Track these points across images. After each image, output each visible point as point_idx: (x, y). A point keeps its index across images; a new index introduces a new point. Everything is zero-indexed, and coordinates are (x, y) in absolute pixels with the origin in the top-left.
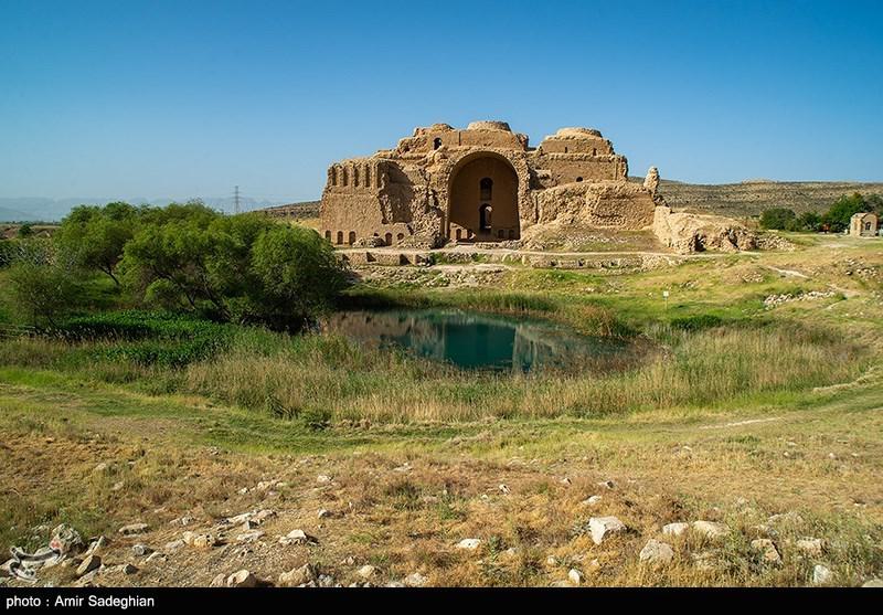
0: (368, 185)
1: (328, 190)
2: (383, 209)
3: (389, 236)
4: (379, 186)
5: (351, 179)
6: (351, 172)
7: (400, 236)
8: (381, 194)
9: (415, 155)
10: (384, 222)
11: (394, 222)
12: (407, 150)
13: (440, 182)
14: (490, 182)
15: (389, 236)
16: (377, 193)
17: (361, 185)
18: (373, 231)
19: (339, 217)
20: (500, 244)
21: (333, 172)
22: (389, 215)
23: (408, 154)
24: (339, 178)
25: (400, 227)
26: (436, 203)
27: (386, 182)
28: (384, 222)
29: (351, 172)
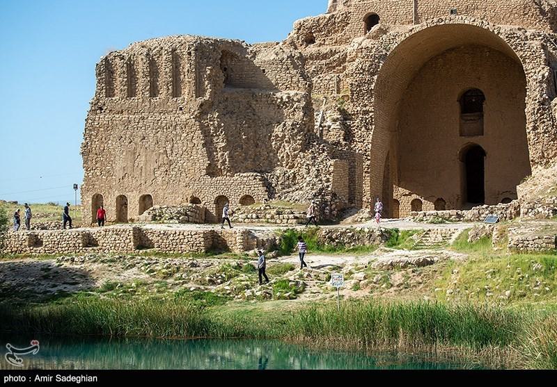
0: (176, 93)
1: (97, 108)
2: (208, 144)
3: (221, 201)
4: (199, 92)
5: (142, 82)
6: (141, 67)
7: (247, 200)
8: (204, 110)
9: (325, 50)
10: (212, 171)
11: (234, 169)
12: (310, 40)
13: (357, 92)
14: (480, 97)
15: (221, 201)
16: (195, 105)
17: (163, 93)
18: (189, 193)
19: (119, 165)
20: (468, 214)
21: (106, 70)
22: (222, 156)
23: (312, 49)
24: (120, 81)
25: (247, 182)
26: (349, 136)
27: (214, 84)
28: (212, 171)
29: (141, 67)
